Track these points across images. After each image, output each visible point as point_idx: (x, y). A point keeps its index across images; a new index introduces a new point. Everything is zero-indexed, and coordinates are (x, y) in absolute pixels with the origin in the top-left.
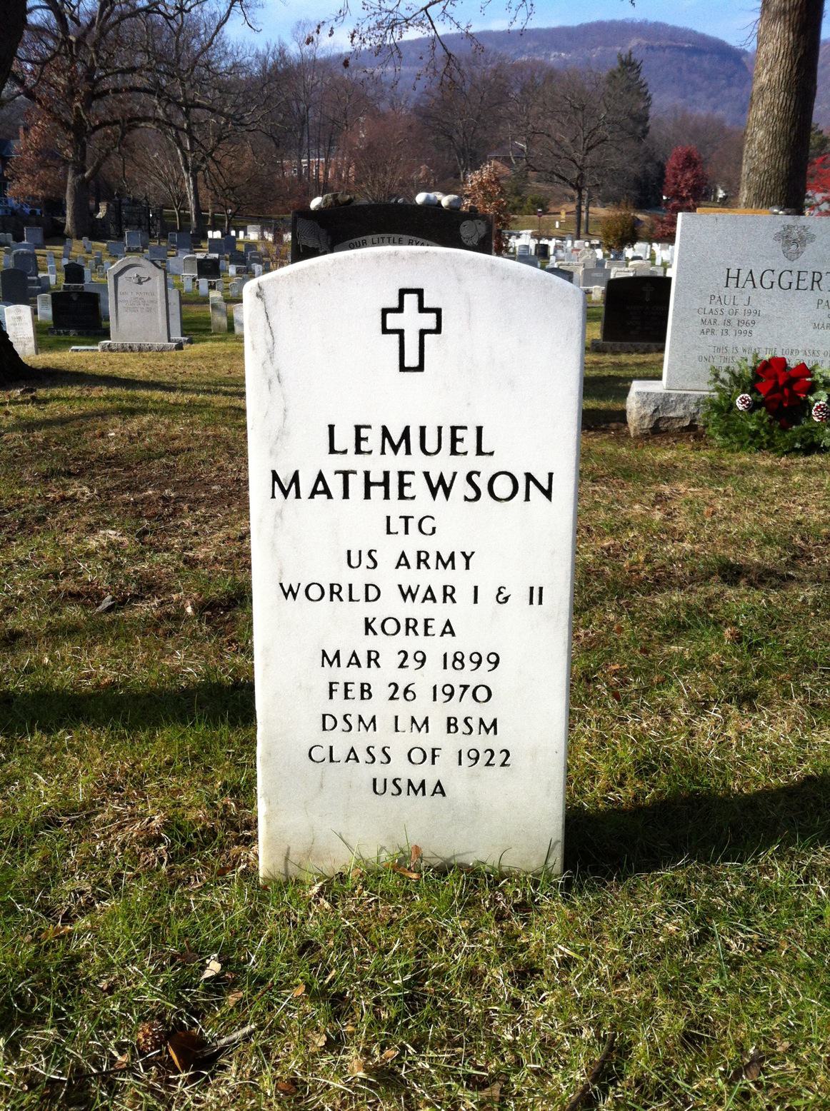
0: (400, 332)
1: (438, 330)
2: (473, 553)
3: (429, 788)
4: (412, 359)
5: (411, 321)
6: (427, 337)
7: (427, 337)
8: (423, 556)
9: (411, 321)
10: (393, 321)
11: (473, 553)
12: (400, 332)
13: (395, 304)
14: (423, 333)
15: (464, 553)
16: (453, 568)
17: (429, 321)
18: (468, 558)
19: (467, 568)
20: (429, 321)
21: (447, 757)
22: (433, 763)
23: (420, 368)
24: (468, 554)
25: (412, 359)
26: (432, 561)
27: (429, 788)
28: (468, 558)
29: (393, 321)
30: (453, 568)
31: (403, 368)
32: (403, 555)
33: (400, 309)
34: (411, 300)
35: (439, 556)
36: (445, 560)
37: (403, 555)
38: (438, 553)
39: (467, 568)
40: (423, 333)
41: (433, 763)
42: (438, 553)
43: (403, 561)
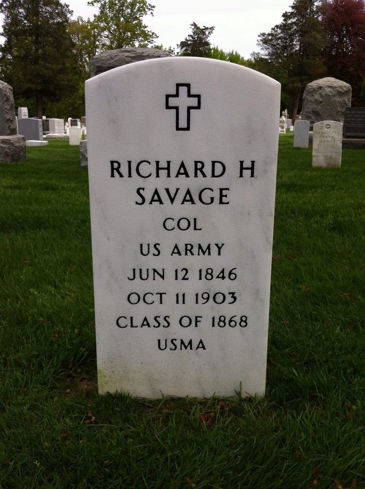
0: (177, 108)
1: (198, 107)
2: (223, 245)
3: (195, 344)
4: (183, 123)
5: (183, 101)
6: (192, 111)
7: (192, 111)
8: (189, 247)
9: (183, 101)
10: (173, 102)
11: (223, 245)
12: (177, 108)
13: (174, 93)
14: (189, 108)
15: (217, 245)
16: (209, 254)
17: (193, 102)
18: (219, 249)
19: (219, 254)
20: (193, 102)
21: (206, 323)
22: (196, 326)
23: (188, 129)
24: (220, 246)
25: (183, 123)
26: (195, 250)
27: (195, 344)
28: (219, 249)
29: (173, 102)
30: (209, 254)
31: (178, 129)
32: (176, 247)
33: (177, 95)
34: (183, 90)
35: (200, 247)
36: (204, 249)
37: (176, 247)
38: (199, 245)
39: (219, 254)
40: (189, 108)
41: (196, 326)
42: (199, 245)
43: (176, 250)
